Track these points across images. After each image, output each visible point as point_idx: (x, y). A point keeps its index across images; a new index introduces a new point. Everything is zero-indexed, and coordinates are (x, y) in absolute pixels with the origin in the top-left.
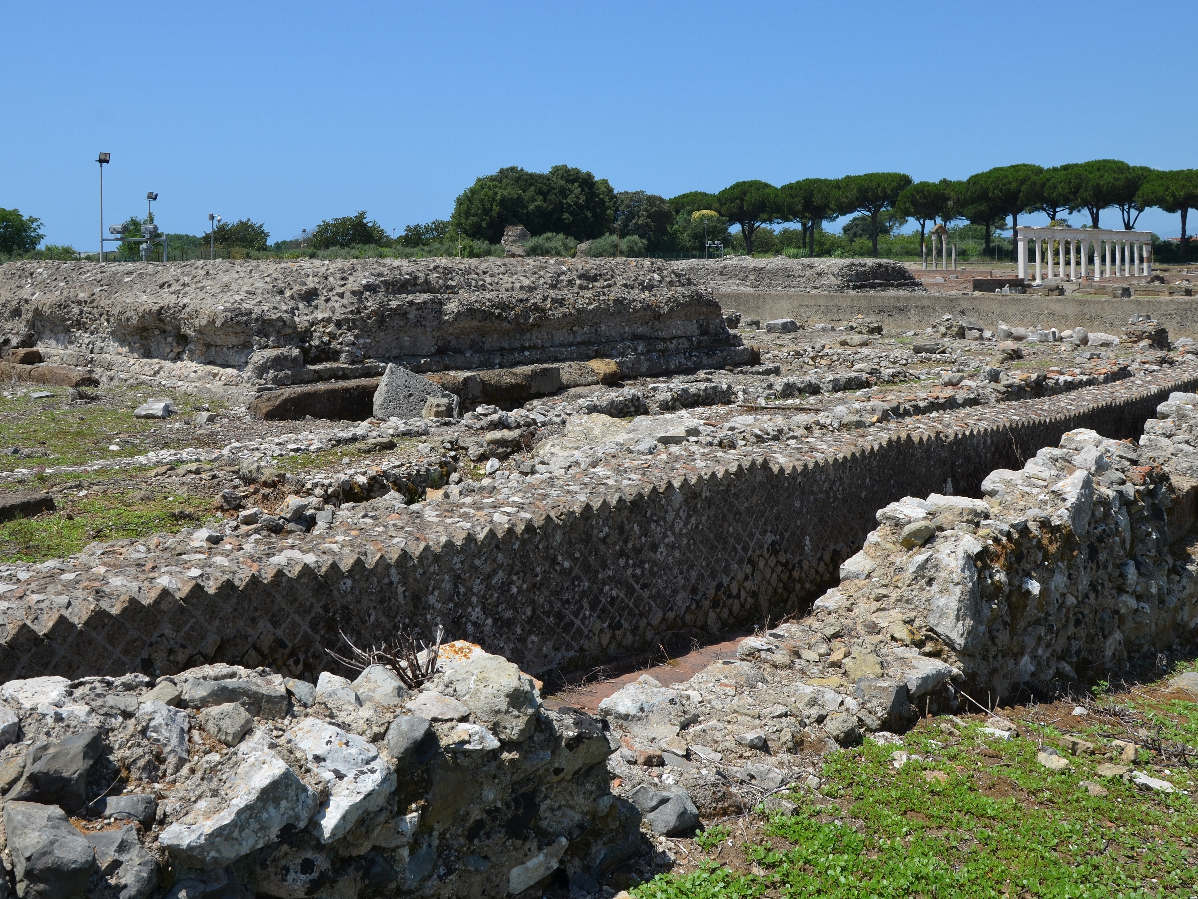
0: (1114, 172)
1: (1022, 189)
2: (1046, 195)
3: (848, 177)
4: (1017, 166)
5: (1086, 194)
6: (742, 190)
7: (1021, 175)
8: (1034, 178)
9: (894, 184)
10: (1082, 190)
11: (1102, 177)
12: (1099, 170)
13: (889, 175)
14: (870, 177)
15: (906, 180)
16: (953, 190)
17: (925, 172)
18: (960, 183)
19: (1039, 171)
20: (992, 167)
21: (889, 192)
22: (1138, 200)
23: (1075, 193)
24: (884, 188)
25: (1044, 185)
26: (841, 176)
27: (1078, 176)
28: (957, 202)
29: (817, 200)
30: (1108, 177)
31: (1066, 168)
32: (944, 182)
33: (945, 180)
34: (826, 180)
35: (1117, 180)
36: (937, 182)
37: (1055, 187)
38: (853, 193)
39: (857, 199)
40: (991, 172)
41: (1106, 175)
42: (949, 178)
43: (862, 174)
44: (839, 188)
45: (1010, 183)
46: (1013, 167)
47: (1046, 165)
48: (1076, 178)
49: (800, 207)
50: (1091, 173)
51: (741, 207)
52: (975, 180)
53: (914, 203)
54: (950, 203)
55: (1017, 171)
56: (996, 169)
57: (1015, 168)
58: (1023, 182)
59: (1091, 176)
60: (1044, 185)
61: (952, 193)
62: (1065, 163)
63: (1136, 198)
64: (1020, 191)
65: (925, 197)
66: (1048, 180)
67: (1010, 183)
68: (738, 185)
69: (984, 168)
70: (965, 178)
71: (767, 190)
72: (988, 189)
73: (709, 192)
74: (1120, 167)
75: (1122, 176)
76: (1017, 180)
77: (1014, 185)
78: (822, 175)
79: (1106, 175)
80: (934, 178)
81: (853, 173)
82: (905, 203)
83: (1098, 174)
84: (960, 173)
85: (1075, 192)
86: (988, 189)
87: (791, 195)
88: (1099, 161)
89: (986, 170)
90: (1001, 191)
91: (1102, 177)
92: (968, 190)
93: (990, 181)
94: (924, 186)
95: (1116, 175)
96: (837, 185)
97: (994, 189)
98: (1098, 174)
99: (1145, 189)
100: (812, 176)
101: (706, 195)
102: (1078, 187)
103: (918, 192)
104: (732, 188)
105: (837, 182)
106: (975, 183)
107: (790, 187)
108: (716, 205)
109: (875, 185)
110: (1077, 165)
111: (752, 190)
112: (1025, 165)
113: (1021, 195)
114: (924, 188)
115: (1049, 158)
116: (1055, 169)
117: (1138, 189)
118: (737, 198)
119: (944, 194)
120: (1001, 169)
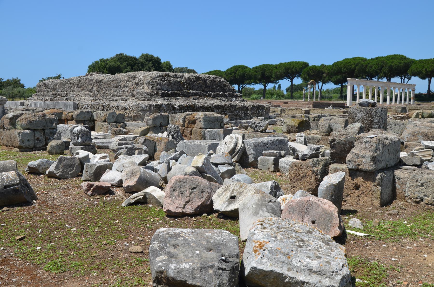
0: (399, 59)
1: (357, 68)
2: (367, 71)
3: (281, 64)
4: (355, 58)
5: (385, 70)
6: (235, 69)
7: (357, 61)
8: (362, 63)
9: (301, 66)
10: (384, 68)
11: (393, 62)
12: (392, 59)
13: (299, 62)
14: (290, 63)
15: (306, 65)
16: (326, 69)
17: (314, 61)
18: (330, 66)
19: (365, 60)
20: (344, 58)
21: (298, 70)
22: (409, 72)
23: (380, 69)
24: (296, 68)
25: (367, 66)
26: (278, 63)
27: (382, 62)
28: (328, 74)
29: (267, 74)
30: (396, 62)
31: (377, 58)
32: (323, 65)
33: (323, 65)
34: (272, 65)
35: (400, 63)
36: (319, 65)
37: (371, 67)
38: (282, 70)
39: (284, 73)
40: (343, 60)
41: (395, 61)
42: (325, 64)
43: (287, 62)
44: (277, 68)
45: (351, 65)
46: (353, 58)
47: (368, 57)
48: (381, 62)
49: (259, 77)
50: (388, 60)
51: (235, 77)
52: (336, 64)
53: (309, 75)
54: (325, 75)
55: (355, 60)
56: (345, 59)
57: (354, 59)
58: (357, 65)
59: (388, 62)
60: (367, 66)
61: (326, 71)
62: (376, 56)
63: (408, 72)
64: (356, 69)
65: (313, 72)
66: (369, 64)
67: (351, 65)
68: (234, 67)
69: (341, 59)
70: (331, 64)
71: (246, 69)
72: (341, 68)
73: (222, 70)
74: (403, 58)
75: (403, 62)
76: (355, 64)
77: (353, 66)
78: (270, 63)
79: (395, 61)
80: (318, 63)
81: (283, 62)
82: (304, 75)
83: (391, 61)
84: (329, 62)
85: (380, 69)
86: (341, 68)
87: (256, 72)
88: (393, 55)
89: (342, 60)
90: (347, 69)
91: (393, 62)
92: (332, 69)
93: (342, 65)
94: (314, 67)
95: (400, 61)
96: (276, 67)
97: (344, 68)
98: (391, 61)
99: (413, 68)
100: (266, 63)
102: (382, 67)
103: (311, 70)
104: (231, 68)
105: (276, 65)
106: (336, 65)
107: (256, 68)
108: (224, 76)
109: (292, 66)
110: (382, 57)
111: (240, 69)
112: (359, 57)
113: (356, 71)
114: (314, 68)
115: (370, 54)
116: (372, 59)
117: (409, 67)
118: (233, 73)
119: (322, 71)
120: (348, 59)
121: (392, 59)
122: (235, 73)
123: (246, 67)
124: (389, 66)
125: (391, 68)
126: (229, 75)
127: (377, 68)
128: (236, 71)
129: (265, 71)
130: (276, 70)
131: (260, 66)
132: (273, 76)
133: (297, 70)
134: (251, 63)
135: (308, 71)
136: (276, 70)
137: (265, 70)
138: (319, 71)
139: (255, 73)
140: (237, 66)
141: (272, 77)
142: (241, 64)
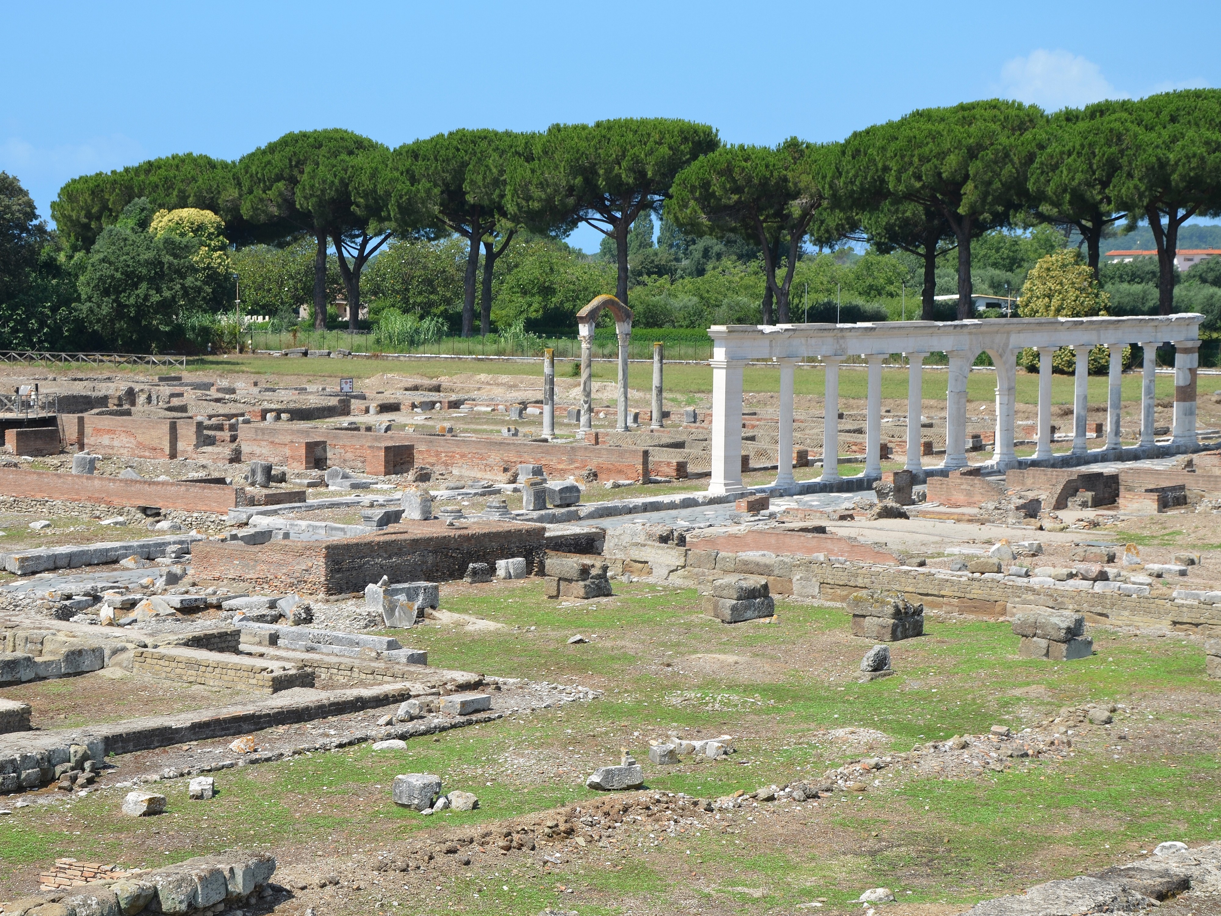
6: (295, 154)
9: (664, 150)
24: (637, 160)
25: (1031, 158)
45: (942, 155)
50: (1149, 128)
52: (859, 145)
55: (967, 121)
60: (1031, 158)
64: (966, 177)
66: (1041, 147)
71: (360, 160)
101: (212, 165)
102: (1112, 167)
104: (272, 148)
106: (856, 153)
109: (614, 152)
121: (1173, 119)
122: (293, 181)
123: (361, 145)
124: (1150, 169)
125: (1159, 174)
126: (258, 192)
127: (1079, 176)
128: (300, 164)
129: (459, 173)
130: (522, 171)
131: (437, 142)
132: (511, 208)
133: (642, 174)
134: (397, 114)
135: (706, 185)
136: (522, 171)
137: (464, 165)
138: (764, 182)
139: (404, 186)
140: (304, 135)
141: (504, 214)
142: (330, 125)
